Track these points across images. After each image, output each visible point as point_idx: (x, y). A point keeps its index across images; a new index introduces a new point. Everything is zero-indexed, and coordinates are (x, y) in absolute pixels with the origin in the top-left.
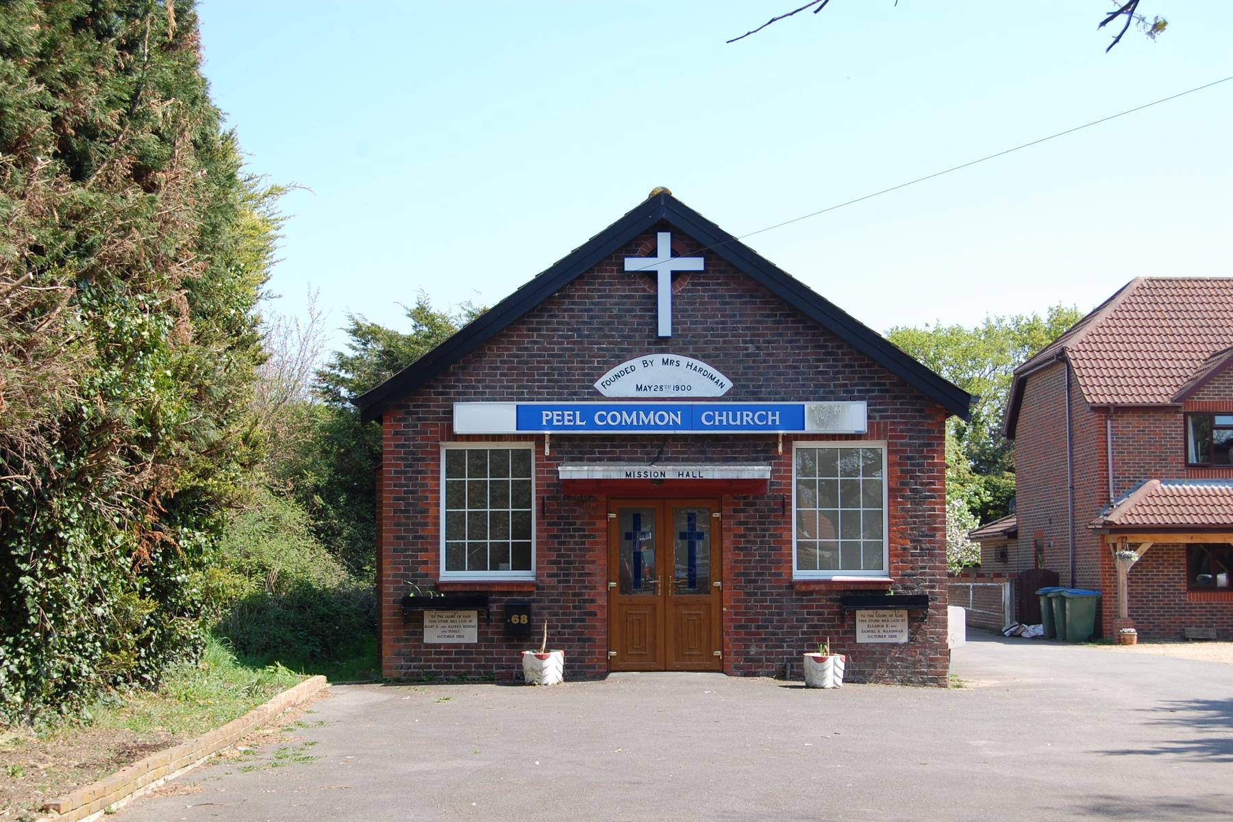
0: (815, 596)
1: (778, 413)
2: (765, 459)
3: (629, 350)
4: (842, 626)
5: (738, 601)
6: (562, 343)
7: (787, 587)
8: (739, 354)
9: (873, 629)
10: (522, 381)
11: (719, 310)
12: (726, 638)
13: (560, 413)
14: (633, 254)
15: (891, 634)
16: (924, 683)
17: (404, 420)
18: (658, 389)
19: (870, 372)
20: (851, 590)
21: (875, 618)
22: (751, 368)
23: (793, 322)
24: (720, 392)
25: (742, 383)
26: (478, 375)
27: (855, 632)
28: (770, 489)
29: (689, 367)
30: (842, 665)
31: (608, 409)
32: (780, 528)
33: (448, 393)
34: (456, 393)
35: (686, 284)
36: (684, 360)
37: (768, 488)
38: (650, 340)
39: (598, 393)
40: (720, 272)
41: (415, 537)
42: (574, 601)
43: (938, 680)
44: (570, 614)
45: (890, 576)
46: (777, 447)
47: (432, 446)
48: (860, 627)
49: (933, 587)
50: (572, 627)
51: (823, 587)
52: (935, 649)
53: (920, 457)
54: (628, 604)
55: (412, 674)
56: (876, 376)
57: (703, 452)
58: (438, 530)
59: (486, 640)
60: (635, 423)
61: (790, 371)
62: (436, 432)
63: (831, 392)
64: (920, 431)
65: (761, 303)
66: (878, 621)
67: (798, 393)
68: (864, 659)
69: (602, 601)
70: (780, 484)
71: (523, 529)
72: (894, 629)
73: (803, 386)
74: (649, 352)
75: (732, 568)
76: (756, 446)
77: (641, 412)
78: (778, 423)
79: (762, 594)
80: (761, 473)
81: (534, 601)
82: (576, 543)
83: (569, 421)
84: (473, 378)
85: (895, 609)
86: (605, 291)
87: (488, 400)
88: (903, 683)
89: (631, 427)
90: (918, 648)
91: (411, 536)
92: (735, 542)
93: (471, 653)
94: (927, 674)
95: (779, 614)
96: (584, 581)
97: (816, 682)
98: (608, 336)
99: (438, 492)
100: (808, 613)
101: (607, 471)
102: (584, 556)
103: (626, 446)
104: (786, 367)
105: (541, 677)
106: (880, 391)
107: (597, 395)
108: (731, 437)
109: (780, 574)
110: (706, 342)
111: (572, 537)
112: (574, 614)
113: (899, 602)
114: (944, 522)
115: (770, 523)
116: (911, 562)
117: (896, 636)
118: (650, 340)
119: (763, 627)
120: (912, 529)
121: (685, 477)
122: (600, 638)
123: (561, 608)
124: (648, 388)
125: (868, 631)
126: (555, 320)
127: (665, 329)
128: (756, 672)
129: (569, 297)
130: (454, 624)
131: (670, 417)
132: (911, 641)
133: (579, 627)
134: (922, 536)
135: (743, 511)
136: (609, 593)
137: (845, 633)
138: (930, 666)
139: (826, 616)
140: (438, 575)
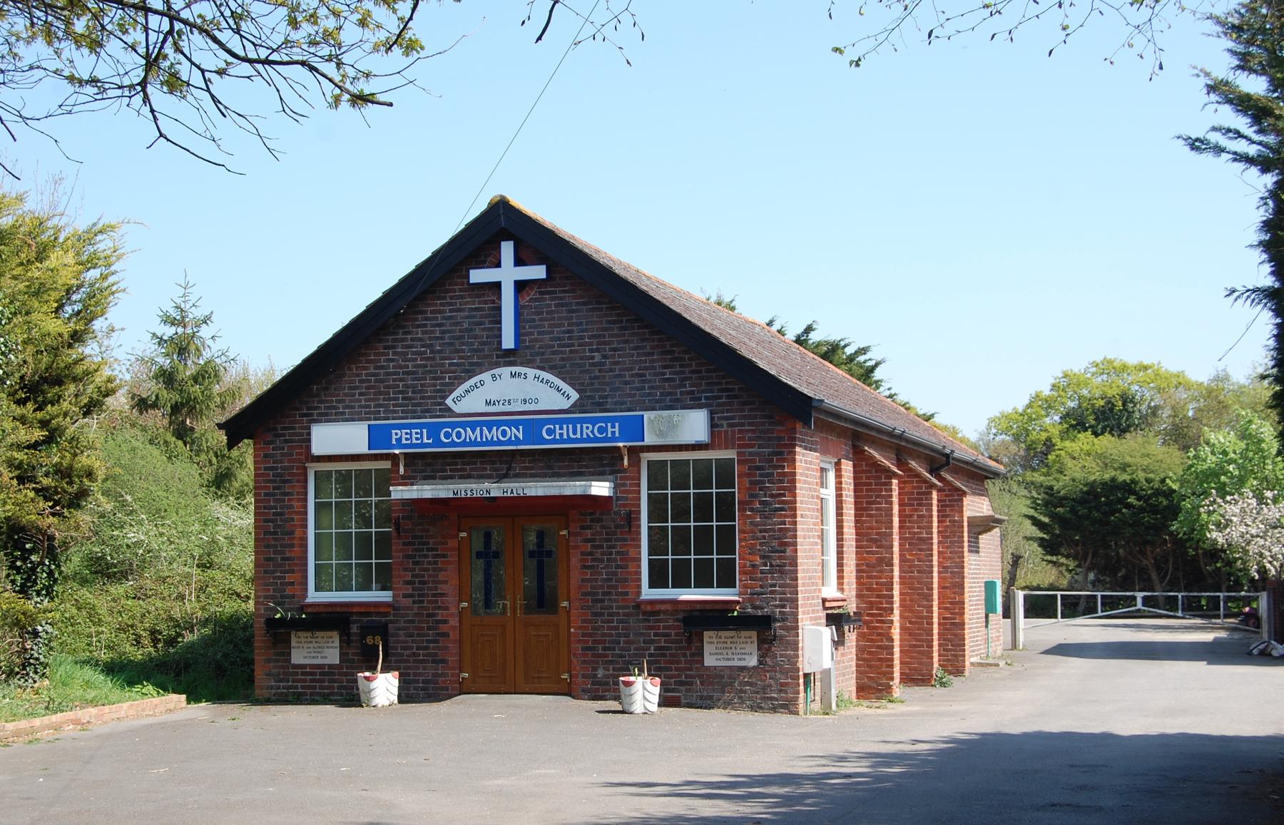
1: (617, 424)
2: (612, 473)
3: (478, 364)
4: (689, 648)
5: (585, 621)
6: (415, 360)
7: (634, 607)
8: (585, 363)
9: (720, 651)
10: (379, 399)
12: (574, 660)
15: (739, 656)
16: (774, 710)
18: (506, 403)
21: (723, 640)
22: (598, 378)
23: (639, 328)
24: (566, 404)
25: (589, 394)
26: (338, 395)
27: (701, 654)
28: (616, 505)
30: (657, 690)
32: (626, 545)
35: (533, 294)
36: (531, 372)
38: (499, 353)
39: (449, 409)
41: (283, 559)
42: (428, 622)
43: (789, 707)
44: (424, 635)
45: (740, 594)
46: (623, 460)
47: (298, 468)
48: (708, 649)
49: (784, 606)
50: (426, 648)
51: (669, 607)
52: (785, 673)
53: (769, 466)
56: (724, 381)
57: (550, 467)
58: (306, 552)
60: (479, 439)
62: (301, 454)
63: (678, 400)
64: (769, 439)
67: (644, 403)
68: (712, 684)
69: (454, 622)
70: (627, 499)
72: (743, 651)
73: (649, 394)
74: (497, 365)
75: (579, 587)
76: (601, 459)
78: (617, 435)
79: (609, 615)
80: (583, 489)
81: (391, 622)
82: (429, 563)
83: (417, 439)
87: (347, 420)
88: (756, 708)
89: (475, 443)
90: (768, 671)
91: (279, 557)
92: (582, 560)
93: (333, 674)
94: (777, 700)
95: (626, 635)
97: (626, 708)
98: (457, 351)
99: (306, 513)
103: (475, 463)
104: (633, 376)
105: (369, 699)
106: (728, 397)
107: (448, 411)
109: (626, 594)
110: (554, 353)
111: (426, 556)
114: (795, 537)
115: (616, 540)
116: (761, 579)
117: (745, 659)
118: (499, 353)
120: (761, 544)
121: (509, 495)
122: (452, 659)
123: (416, 628)
125: (716, 654)
126: (409, 337)
127: (508, 342)
130: (317, 645)
131: (513, 432)
133: (434, 648)
135: (589, 528)
136: (461, 613)
137: (693, 655)
139: (673, 637)
140: (639, 593)
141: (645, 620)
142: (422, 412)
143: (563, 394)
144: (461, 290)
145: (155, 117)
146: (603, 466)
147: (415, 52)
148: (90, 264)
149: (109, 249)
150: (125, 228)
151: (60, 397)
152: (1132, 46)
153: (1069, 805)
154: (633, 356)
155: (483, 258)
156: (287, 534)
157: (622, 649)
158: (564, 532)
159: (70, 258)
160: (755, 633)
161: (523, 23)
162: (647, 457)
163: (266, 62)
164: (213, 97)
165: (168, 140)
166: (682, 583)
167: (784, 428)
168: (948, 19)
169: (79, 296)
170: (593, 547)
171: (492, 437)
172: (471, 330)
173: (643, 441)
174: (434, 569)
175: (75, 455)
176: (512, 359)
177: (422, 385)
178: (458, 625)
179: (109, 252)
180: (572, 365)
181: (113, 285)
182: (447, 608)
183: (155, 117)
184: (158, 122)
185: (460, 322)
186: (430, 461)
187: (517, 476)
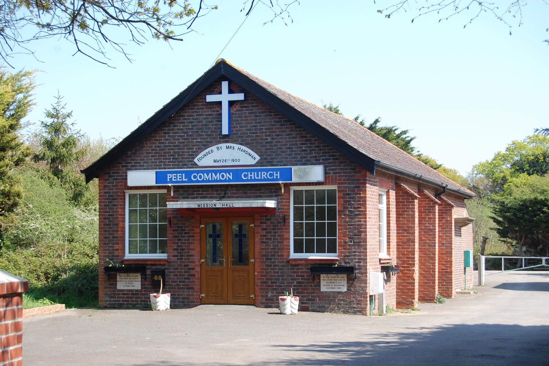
0: (300, 267)
1: (279, 172)
5: (262, 269)
6: (179, 139)
8: (263, 142)
9: (328, 284)
10: (161, 159)
13: (176, 175)
14: (212, 93)
15: (338, 287)
16: (355, 313)
17: (108, 180)
19: (328, 149)
20: (318, 264)
21: (330, 278)
23: (290, 125)
24: (253, 162)
25: (265, 157)
26: (141, 157)
27: (320, 286)
28: (278, 212)
29: (239, 150)
30: (297, 303)
31: (198, 172)
32: (284, 232)
35: (237, 107)
36: (236, 146)
37: (277, 211)
38: (220, 136)
39: (196, 164)
40: (254, 100)
41: (113, 237)
42: (185, 269)
43: (362, 311)
44: (183, 275)
45: (338, 256)
46: (281, 189)
48: (322, 283)
49: (360, 262)
50: (184, 282)
51: (303, 262)
52: (360, 295)
53: (353, 193)
54: (210, 271)
55: (112, 304)
56: (331, 151)
57: (245, 193)
58: (124, 234)
59: (145, 288)
60: (210, 179)
61: (288, 150)
62: (122, 185)
63: (309, 160)
64: (354, 180)
65: (274, 115)
66: (332, 280)
67: (292, 162)
68: (324, 300)
69: (198, 269)
70: (283, 209)
72: (340, 284)
73: (295, 158)
74: (220, 142)
75: (259, 252)
76: (271, 189)
77: (213, 174)
78: (279, 177)
79: (274, 266)
80: (262, 204)
81: (166, 269)
82: (185, 240)
83: (180, 179)
86: (199, 112)
88: (346, 312)
90: (352, 294)
92: (261, 239)
93: (138, 294)
94: (356, 308)
95: (282, 276)
96: (189, 259)
97: (282, 311)
98: (200, 135)
99: (124, 215)
100: (297, 276)
102: (189, 246)
103: (209, 191)
104: (286, 148)
105: (156, 307)
106: (333, 159)
108: (259, 185)
109: (283, 256)
110: (247, 137)
111: (184, 237)
112: (185, 275)
113: (341, 270)
114: (366, 228)
115: (278, 229)
116: (349, 249)
117: (341, 288)
118: (220, 136)
120: (349, 232)
121: (225, 207)
122: (197, 287)
123: (178, 272)
125: (326, 285)
126: (176, 128)
127: (225, 131)
128: (271, 306)
129: (183, 116)
130: (130, 280)
132: (348, 290)
133: (188, 282)
134: (354, 236)
135: (265, 223)
137: (315, 286)
138: (358, 304)
139: (305, 277)
140: (289, 255)
141: (291, 269)
142: (182, 165)
144: (202, 105)
145: (76, 43)
146: (272, 192)
147: (191, 15)
148: (19, 90)
149: (28, 83)
150: (36, 73)
151: (4, 157)
152: (510, 12)
153: (490, 355)
158: (252, 225)
159: (9, 89)
161: (241, 10)
162: (293, 188)
163: (128, 21)
164: (102, 34)
165: (82, 52)
166: (310, 250)
167: (361, 175)
168: (420, 15)
169: (13, 107)
170: (267, 232)
171: (217, 178)
172: (207, 125)
173: (292, 180)
174: (188, 243)
175: (12, 186)
176: (227, 139)
177: (182, 152)
178: (200, 270)
179: (28, 85)
180: (257, 143)
181: (30, 101)
182: (194, 262)
183: (76, 43)
184: (78, 45)
185: (201, 121)
186: (186, 189)
187: (229, 197)
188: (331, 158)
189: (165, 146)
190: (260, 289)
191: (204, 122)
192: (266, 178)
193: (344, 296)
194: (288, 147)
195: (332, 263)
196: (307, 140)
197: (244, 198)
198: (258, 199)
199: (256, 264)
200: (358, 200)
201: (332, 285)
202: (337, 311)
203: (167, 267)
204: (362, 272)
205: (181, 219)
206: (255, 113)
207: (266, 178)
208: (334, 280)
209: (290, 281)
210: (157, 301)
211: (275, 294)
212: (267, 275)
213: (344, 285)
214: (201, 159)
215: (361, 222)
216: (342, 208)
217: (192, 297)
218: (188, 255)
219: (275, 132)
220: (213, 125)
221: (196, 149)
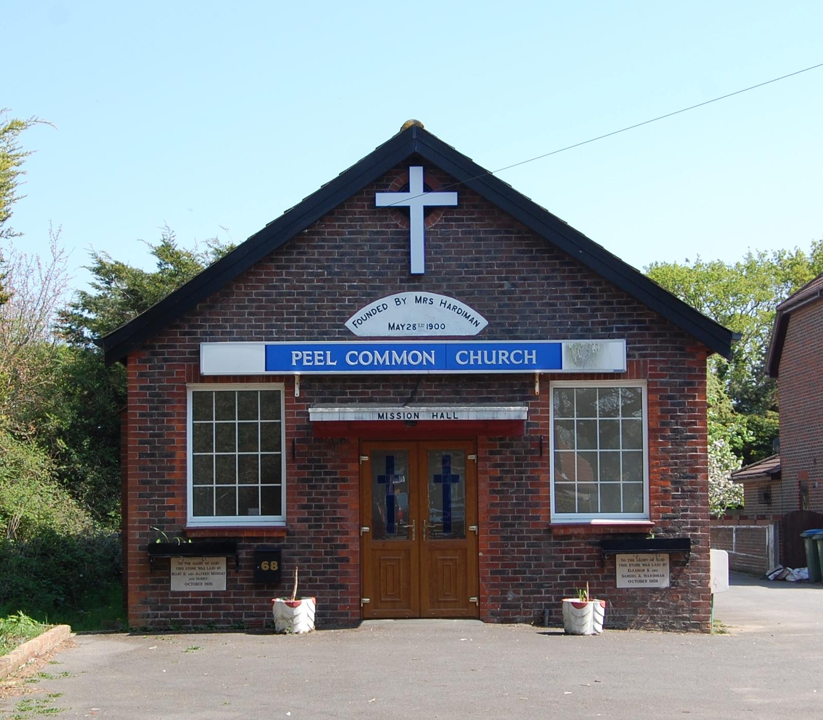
0: (573, 540)
1: (534, 352)
3: (379, 288)
7: (545, 531)
8: (494, 291)
10: (271, 320)
11: (473, 246)
13: (311, 353)
14: (384, 189)
15: (652, 578)
16: (686, 629)
17: (149, 361)
18: (411, 328)
21: (635, 562)
23: (549, 258)
24: (475, 331)
25: (498, 321)
26: (225, 314)
28: (527, 430)
29: (443, 305)
31: (360, 348)
33: (195, 333)
34: (205, 333)
35: (439, 220)
36: (437, 298)
37: (525, 429)
38: (402, 277)
39: (349, 332)
40: (475, 207)
41: (161, 482)
42: (325, 547)
43: (700, 625)
44: (321, 560)
45: (651, 519)
46: (534, 387)
47: (179, 388)
48: (620, 571)
49: (695, 530)
51: (582, 531)
52: (697, 594)
53: (681, 396)
54: (382, 550)
57: (458, 393)
58: (185, 475)
60: (388, 363)
61: (547, 309)
63: (589, 330)
64: (680, 370)
66: (639, 565)
67: (556, 332)
69: (354, 546)
70: (537, 425)
71: (272, 474)
72: (656, 573)
73: (560, 324)
74: (401, 290)
75: (488, 512)
76: (512, 386)
78: (534, 362)
79: (520, 538)
80: (517, 414)
81: (284, 547)
82: (327, 487)
83: (320, 361)
84: (220, 318)
85: (656, 552)
86: (356, 227)
88: (664, 628)
89: (384, 367)
90: (680, 592)
91: (157, 480)
92: (491, 485)
93: (219, 601)
94: (689, 620)
95: (537, 559)
96: (335, 526)
97: (576, 628)
99: (185, 435)
100: (567, 558)
101: (359, 412)
102: (335, 500)
103: (378, 387)
104: (543, 305)
105: (292, 625)
106: (639, 328)
107: (349, 334)
108: (487, 377)
109: (537, 518)
110: (460, 280)
111: (323, 480)
113: (660, 546)
115: (527, 465)
116: (673, 504)
117: (657, 581)
118: (402, 277)
119: (520, 572)
120: (672, 471)
121: (439, 419)
122: (352, 584)
123: (312, 553)
124: (400, 327)
126: (304, 257)
127: (418, 265)
128: (514, 619)
129: (319, 233)
130: (202, 571)
133: (331, 574)
135: (499, 453)
137: (605, 577)
138: (692, 611)
139: (585, 560)
140: (185, 520)
141: (556, 544)
142: (319, 334)
143: (471, 320)
144: (361, 213)
146: (514, 392)
154: (543, 285)
155: (385, 182)
156: (167, 456)
157: (533, 573)
158: (472, 457)
160: (667, 555)
167: (695, 360)
171: (385, 361)
172: (373, 254)
173: (561, 368)
174: (332, 493)
176: (417, 284)
177: (319, 307)
178: (359, 550)
180: (480, 292)
182: (347, 533)
185: (361, 245)
186: (328, 384)
188: (634, 327)
189: (280, 294)
190: (489, 586)
191: (365, 247)
192: (508, 363)
193: (664, 596)
194: (547, 303)
195: (641, 531)
196: (585, 290)
197: (454, 402)
198: (486, 403)
199: (480, 536)
200: (691, 409)
201: (640, 576)
202: (649, 625)
203: (285, 543)
204: (699, 548)
205: (317, 443)
206: (475, 232)
207: (508, 363)
208: (644, 565)
209: (554, 568)
210: (295, 614)
211: (522, 595)
212: (506, 557)
213: (663, 576)
214: (360, 322)
215: (697, 452)
216: (657, 423)
217: (342, 604)
218: (333, 518)
219: (519, 272)
220: (386, 253)
221: (349, 301)
